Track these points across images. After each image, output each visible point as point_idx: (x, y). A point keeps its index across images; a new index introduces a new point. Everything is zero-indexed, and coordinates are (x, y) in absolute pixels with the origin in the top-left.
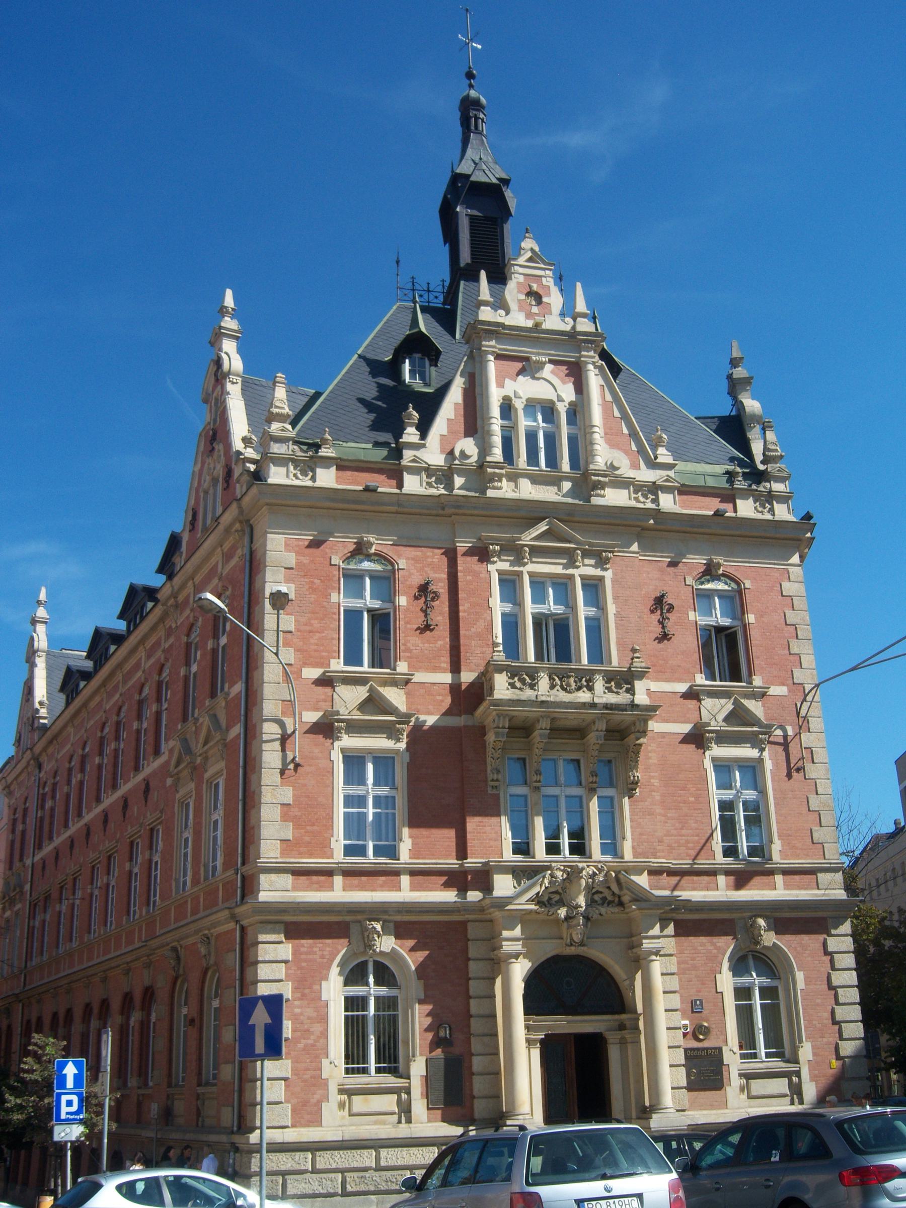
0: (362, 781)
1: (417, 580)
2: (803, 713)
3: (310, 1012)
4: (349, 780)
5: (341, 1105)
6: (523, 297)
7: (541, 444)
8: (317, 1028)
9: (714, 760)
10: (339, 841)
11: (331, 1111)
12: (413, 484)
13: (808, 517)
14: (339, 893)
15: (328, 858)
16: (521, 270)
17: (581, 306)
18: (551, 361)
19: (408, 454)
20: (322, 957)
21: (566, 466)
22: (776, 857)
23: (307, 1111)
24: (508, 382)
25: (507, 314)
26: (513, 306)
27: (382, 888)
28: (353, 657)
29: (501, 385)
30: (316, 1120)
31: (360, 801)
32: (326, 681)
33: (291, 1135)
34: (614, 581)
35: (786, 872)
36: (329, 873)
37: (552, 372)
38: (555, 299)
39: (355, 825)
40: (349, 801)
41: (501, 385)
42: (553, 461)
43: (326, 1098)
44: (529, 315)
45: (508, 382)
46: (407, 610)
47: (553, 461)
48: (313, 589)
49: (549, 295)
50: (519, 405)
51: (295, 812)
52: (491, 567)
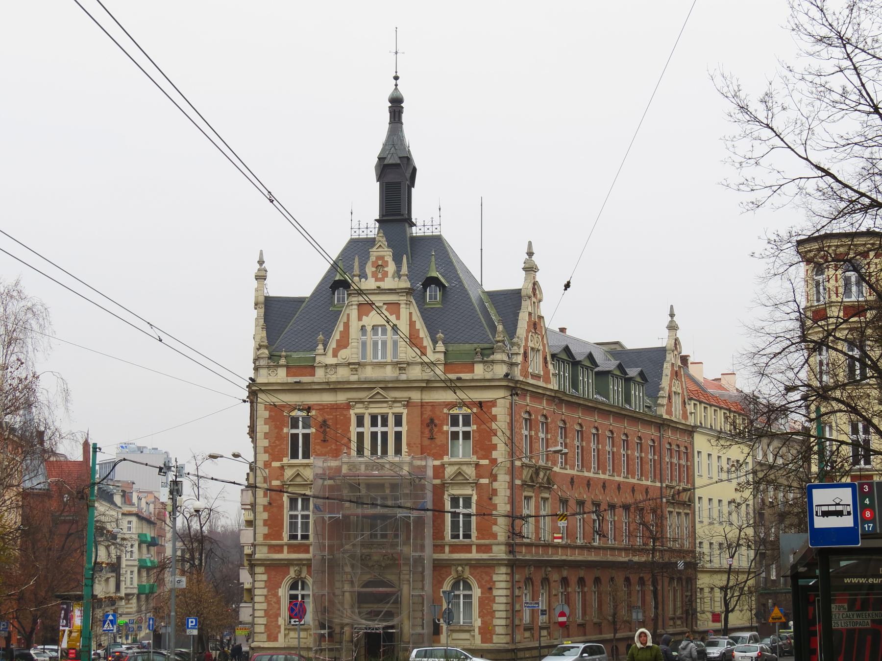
0: (296, 509)
1: (320, 419)
2: (494, 472)
3: (274, 600)
4: (291, 509)
5: (285, 635)
6: (374, 269)
8: (277, 606)
10: (286, 535)
11: (281, 637)
12: (320, 375)
14: (285, 555)
16: (375, 254)
17: (405, 270)
19: (318, 359)
23: (272, 637)
24: (364, 318)
25: (366, 279)
26: (369, 275)
28: (294, 455)
29: (360, 319)
30: (276, 639)
31: (296, 517)
32: (282, 468)
33: (266, 645)
34: (407, 414)
36: (282, 546)
38: (391, 268)
39: (293, 526)
40: (291, 517)
41: (360, 319)
42: (384, 355)
43: (280, 632)
45: (364, 318)
46: (315, 434)
48: (276, 427)
49: (387, 266)
50: (369, 328)
51: (269, 522)
52: (352, 412)
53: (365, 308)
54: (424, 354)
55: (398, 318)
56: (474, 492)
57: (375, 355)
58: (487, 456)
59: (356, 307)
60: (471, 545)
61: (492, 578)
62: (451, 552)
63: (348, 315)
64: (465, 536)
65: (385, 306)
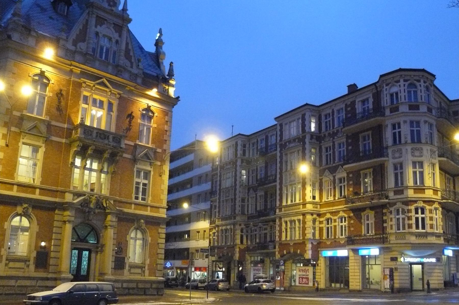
7: (104, 51)
9: (137, 168)
13: (179, 97)
15: (12, 179)
18: (114, 24)
20: (7, 213)
21: (111, 61)
22: (149, 202)
24: (98, 27)
27: (29, 193)
29: (96, 27)
35: (152, 207)
37: (113, 27)
41: (96, 27)
44: (109, 5)
45: (98, 27)
47: (106, 58)
53: (100, 21)
54: (132, 67)
55: (120, 36)
56: (152, 169)
57: (101, 57)
58: (161, 147)
59: (95, 16)
60: (147, 206)
61: (158, 230)
62: (135, 209)
63: (87, 21)
64: (143, 199)
65: (113, 25)
